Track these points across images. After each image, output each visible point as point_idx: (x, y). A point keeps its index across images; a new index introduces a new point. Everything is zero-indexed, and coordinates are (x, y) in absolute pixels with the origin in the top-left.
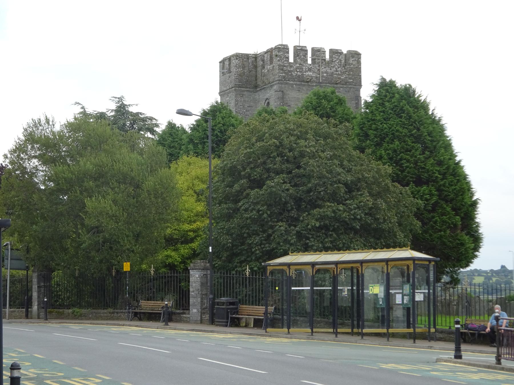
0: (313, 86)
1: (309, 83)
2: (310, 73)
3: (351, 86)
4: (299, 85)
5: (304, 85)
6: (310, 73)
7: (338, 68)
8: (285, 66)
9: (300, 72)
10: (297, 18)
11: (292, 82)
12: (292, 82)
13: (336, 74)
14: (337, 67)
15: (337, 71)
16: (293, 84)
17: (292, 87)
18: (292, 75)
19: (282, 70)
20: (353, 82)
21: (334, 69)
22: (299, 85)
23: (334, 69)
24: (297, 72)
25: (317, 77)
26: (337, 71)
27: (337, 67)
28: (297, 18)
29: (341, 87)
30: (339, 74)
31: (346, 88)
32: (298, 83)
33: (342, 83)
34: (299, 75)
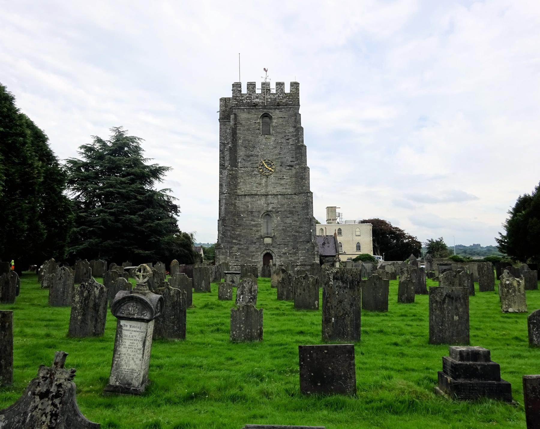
0: (260, 109)
1: (257, 107)
2: (257, 100)
3: (290, 107)
4: (249, 109)
5: (253, 109)
6: (257, 100)
7: (280, 94)
8: (238, 97)
9: (249, 100)
10: (265, 69)
11: (242, 107)
12: (242, 107)
13: (278, 99)
14: (279, 94)
15: (279, 97)
16: (244, 109)
17: (244, 111)
18: (243, 102)
19: (235, 99)
20: (292, 104)
21: (277, 95)
22: (249, 109)
23: (277, 95)
24: (247, 100)
25: (262, 102)
26: (279, 97)
27: (279, 94)
28: (265, 69)
29: (283, 108)
30: (280, 99)
31: (286, 108)
32: (247, 107)
33: (284, 104)
34: (249, 102)
